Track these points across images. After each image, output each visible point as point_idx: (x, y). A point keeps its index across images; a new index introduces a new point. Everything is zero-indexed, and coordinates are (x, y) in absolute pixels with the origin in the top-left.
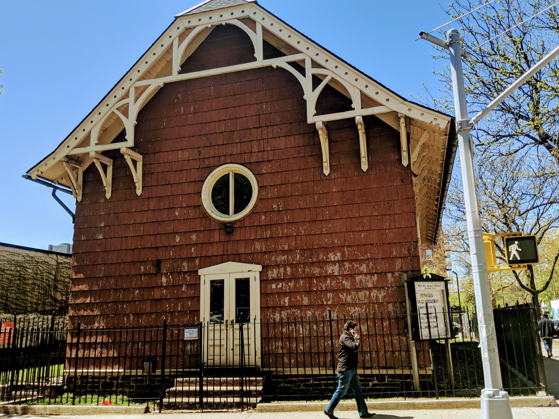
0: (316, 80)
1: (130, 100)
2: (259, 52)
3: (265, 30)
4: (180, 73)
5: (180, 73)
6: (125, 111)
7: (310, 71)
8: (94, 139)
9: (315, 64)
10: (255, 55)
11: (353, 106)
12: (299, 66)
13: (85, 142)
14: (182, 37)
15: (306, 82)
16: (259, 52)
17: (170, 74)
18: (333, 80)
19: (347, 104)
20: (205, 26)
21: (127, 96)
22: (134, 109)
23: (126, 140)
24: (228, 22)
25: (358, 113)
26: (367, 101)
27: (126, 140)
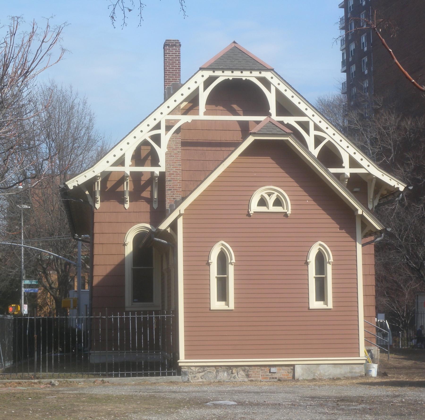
0: (318, 140)
1: (162, 131)
2: (273, 109)
3: (278, 92)
4: (205, 114)
5: (205, 114)
6: (157, 139)
7: (313, 132)
8: (128, 161)
9: (317, 128)
10: (270, 111)
11: (343, 165)
12: (305, 126)
13: (121, 162)
14: (208, 83)
15: (310, 140)
16: (273, 109)
17: (198, 114)
18: (329, 142)
19: (338, 163)
20: (227, 78)
21: (158, 127)
22: (165, 138)
23: (159, 166)
24: (248, 78)
25: (347, 170)
26: (354, 163)
27: (159, 166)
